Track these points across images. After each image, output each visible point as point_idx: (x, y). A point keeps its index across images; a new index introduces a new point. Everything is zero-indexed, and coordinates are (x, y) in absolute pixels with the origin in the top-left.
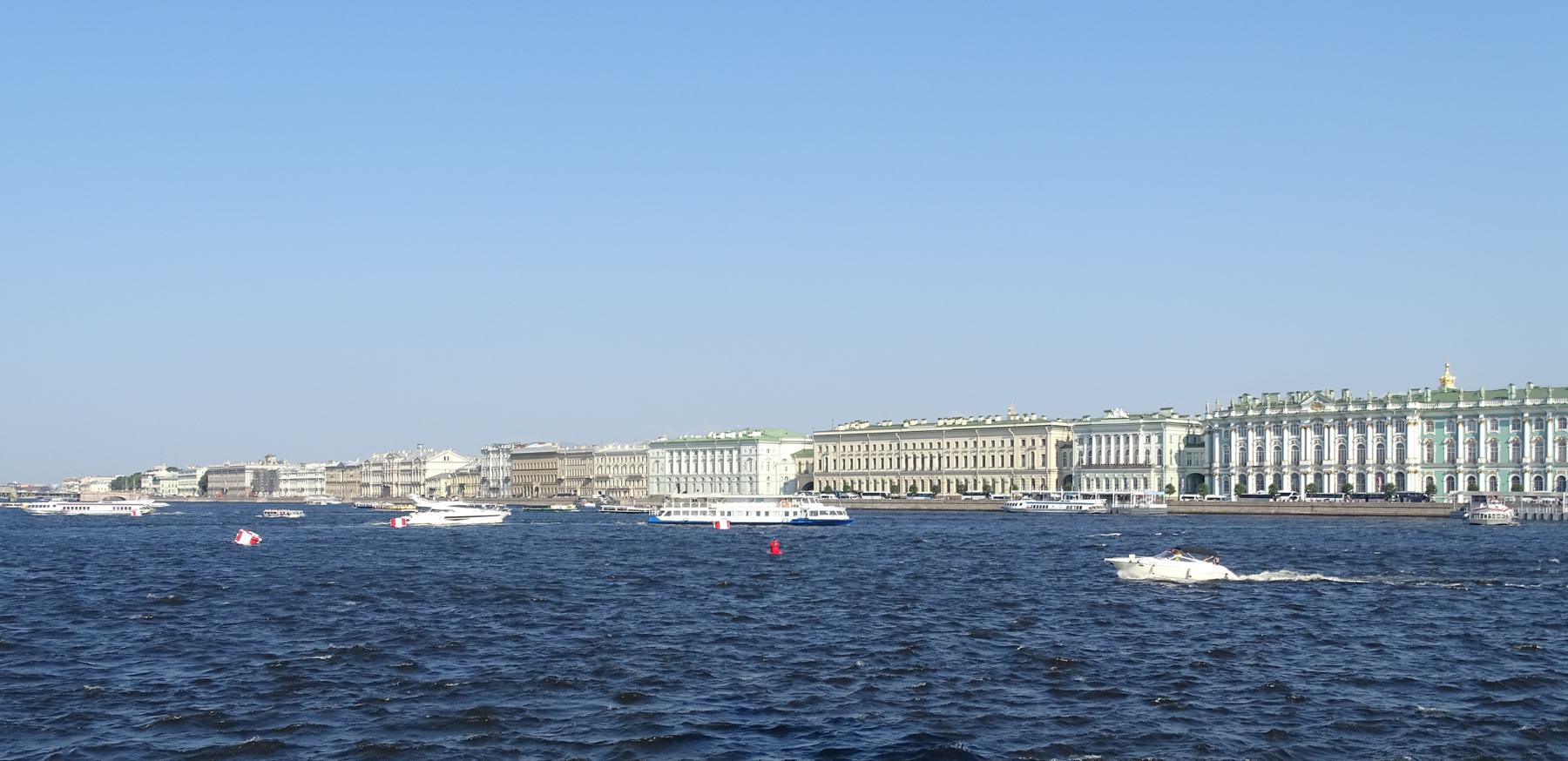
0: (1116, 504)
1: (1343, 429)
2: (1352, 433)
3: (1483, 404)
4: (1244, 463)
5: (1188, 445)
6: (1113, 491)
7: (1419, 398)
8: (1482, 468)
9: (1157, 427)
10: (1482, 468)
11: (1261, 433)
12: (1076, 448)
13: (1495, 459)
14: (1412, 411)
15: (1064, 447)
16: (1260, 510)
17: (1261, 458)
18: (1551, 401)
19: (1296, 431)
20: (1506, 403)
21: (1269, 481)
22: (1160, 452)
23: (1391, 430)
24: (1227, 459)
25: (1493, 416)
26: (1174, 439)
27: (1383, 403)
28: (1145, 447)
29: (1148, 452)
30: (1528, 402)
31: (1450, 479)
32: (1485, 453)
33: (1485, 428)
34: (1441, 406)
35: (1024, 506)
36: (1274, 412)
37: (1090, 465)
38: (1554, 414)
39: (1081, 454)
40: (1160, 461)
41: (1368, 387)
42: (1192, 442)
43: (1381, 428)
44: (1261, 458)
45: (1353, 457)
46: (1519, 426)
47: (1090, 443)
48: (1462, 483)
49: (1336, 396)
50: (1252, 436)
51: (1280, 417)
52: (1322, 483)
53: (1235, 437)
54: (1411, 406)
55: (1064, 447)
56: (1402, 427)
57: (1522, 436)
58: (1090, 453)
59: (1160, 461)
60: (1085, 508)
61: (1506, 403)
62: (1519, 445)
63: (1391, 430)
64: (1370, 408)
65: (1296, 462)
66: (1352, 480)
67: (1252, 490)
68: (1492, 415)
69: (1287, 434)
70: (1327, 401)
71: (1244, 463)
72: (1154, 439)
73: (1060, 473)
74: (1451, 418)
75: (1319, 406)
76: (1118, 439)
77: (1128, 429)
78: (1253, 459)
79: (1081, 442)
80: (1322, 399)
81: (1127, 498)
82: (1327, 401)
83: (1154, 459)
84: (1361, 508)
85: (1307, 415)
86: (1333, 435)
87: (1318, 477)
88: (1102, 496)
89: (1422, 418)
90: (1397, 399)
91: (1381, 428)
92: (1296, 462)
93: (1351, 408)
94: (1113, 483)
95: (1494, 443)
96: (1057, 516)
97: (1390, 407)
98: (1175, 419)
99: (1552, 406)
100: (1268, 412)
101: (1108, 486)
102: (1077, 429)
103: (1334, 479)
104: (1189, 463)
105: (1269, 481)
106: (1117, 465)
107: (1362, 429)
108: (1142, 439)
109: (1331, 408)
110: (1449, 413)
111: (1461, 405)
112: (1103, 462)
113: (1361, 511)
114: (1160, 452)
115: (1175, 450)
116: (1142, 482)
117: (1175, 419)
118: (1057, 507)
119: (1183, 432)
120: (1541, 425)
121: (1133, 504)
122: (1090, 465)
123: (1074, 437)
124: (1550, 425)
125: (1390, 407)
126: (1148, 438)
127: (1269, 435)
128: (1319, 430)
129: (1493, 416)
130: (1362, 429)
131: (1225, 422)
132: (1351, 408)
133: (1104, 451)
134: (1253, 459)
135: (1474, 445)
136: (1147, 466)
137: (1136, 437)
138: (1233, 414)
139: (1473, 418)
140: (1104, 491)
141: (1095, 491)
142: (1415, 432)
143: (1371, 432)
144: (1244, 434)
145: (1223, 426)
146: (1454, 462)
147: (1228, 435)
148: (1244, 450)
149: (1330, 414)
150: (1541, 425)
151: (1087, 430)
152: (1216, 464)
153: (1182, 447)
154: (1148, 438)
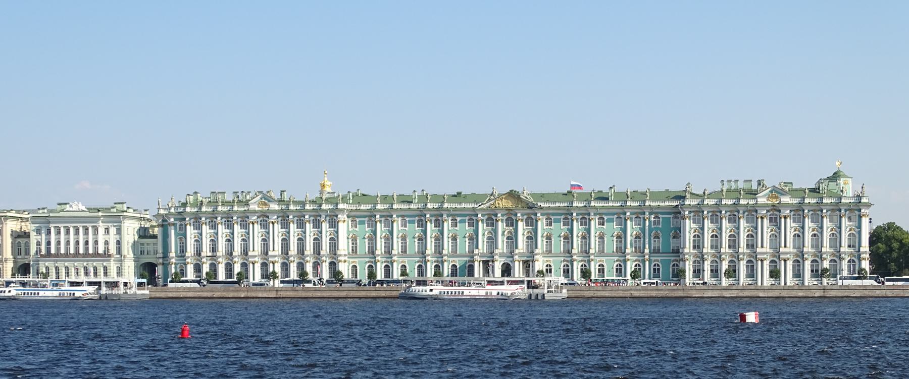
0: (104, 290)
1: (285, 225)
2: (293, 227)
3: (395, 206)
4: (198, 253)
5: (140, 237)
6: (102, 278)
7: (345, 199)
8: (395, 258)
9: (117, 220)
10: (395, 258)
11: (214, 226)
12: (34, 238)
13: (404, 251)
14: (342, 210)
15: (21, 236)
16: (231, 295)
17: (214, 249)
18: (445, 206)
19: (245, 226)
20: (412, 206)
21: (237, 269)
22: (119, 243)
23: (325, 226)
24: (182, 250)
25: (403, 216)
26: (130, 230)
27: (303, 204)
28: (105, 238)
29: (107, 243)
30: (429, 206)
31: (420, 266)
32: (344, 246)
33: (397, 226)
34: (363, 207)
35: (14, 293)
36: (225, 209)
37: (48, 254)
38: (398, 216)
39: (39, 244)
40: (119, 251)
41: (302, 190)
42: (144, 234)
43: (317, 225)
44: (214, 249)
45: (309, 249)
46: (422, 224)
47: (49, 232)
48: (293, 268)
49: (276, 196)
50: (206, 229)
51: (231, 213)
52: (247, 270)
53: (190, 231)
54: (341, 206)
55: (21, 236)
56: (334, 224)
57: (425, 232)
58: (49, 243)
59: (119, 251)
60: (78, 294)
61: (412, 206)
62: (373, 239)
63: (325, 226)
64: (307, 207)
65: (245, 252)
66: (309, 268)
67: (221, 276)
68: (353, 216)
69: (237, 228)
70: (271, 200)
71: (198, 253)
72: (113, 231)
73: (15, 262)
74: (371, 216)
75: (265, 204)
76: (86, 229)
77: (89, 220)
78: (206, 251)
79: (38, 231)
80: (267, 198)
81: (115, 285)
82: (271, 200)
83: (113, 249)
84: (218, 292)
85: (255, 212)
86: (277, 230)
87: (244, 265)
88: (90, 284)
89: (348, 217)
90: (385, 198)
91: (317, 225)
92: (245, 252)
93: (292, 207)
94: (82, 271)
95: (404, 238)
96: (45, 303)
97: (324, 207)
98: (130, 213)
99: (447, 209)
100: (220, 209)
101: (96, 274)
102: (34, 220)
103: (258, 267)
104: (142, 253)
105: (237, 269)
106: (67, 255)
107: (301, 225)
108: (101, 231)
109: (275, 207)
110: (372, 211)
111: (379, 207)
112: (101, 251)
113: (336, 294)
114: (119, 243)
115: (131, 241)
116: (92, 270)
117: (130, 213)
118: (48, 294)
119: (136, 225)
120: (439, 224)
121: (121, 290)
122: (48, 254)
123: (29, 227)
124: (446, 224)
125: (324, 207)
126: (107, 231)
127: (221, 229)
128: (265, 226)
129: (403, 216)
130: (301, 225)
131: (181, 216)
132: (292, 207)
133: (61, 241)
134: (206, 251)
135: (389, 239)
136: (107, 255)
137: (96, 229)
138: (188, 209)
139: (388, 217)
140: (92, 279)
141: (82, 278)
142: (344, 228)
143: (309, 227)
144: (198, 227)
145: (174, 221)
146: (373, 253)
147: (183, 228)
148: (199, 242)
149: (274, 212)
150: (439, 224)
151: (44, 223)
152: (173, 254)
153: (136, 237)
154: (107, 231)
